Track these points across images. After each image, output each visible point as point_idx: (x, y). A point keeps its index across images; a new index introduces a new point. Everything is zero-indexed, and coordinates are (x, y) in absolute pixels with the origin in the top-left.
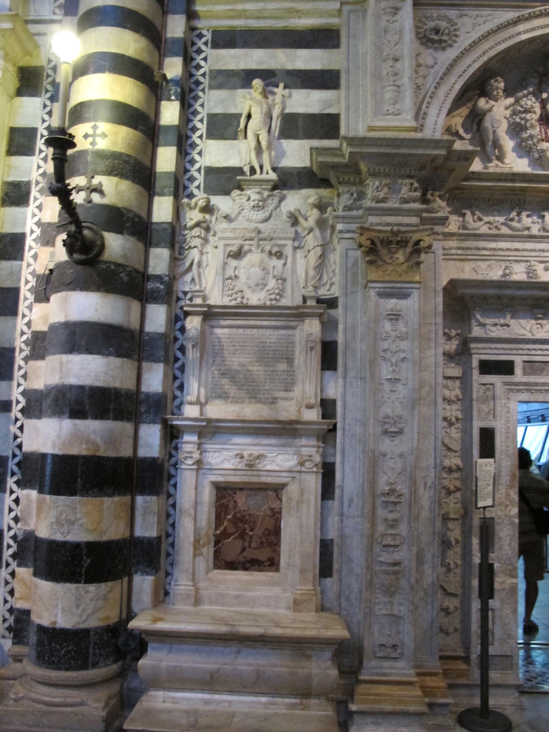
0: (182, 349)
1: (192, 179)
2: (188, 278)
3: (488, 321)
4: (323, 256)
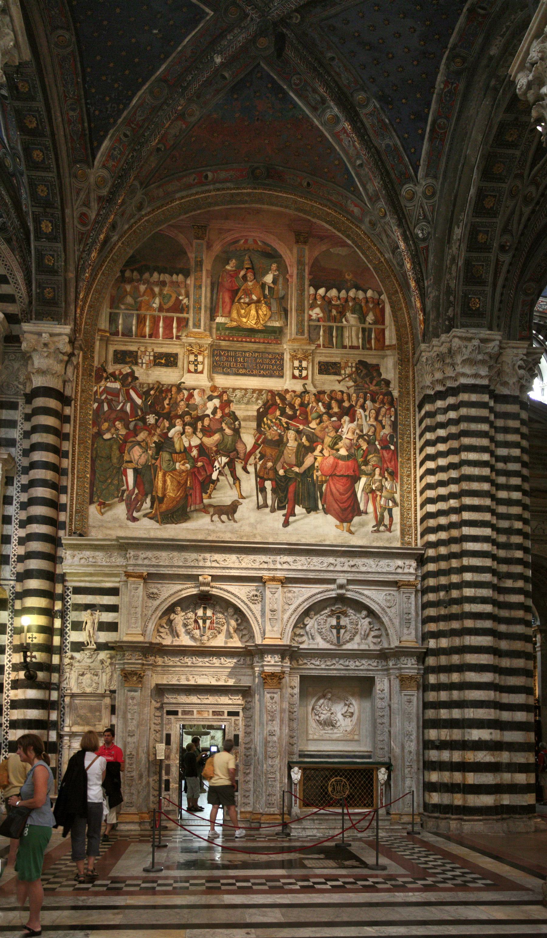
0: (64, 707)
1: (66, 646)
2: (65, 682)
3: (170, 697)
4: (112, 675)
